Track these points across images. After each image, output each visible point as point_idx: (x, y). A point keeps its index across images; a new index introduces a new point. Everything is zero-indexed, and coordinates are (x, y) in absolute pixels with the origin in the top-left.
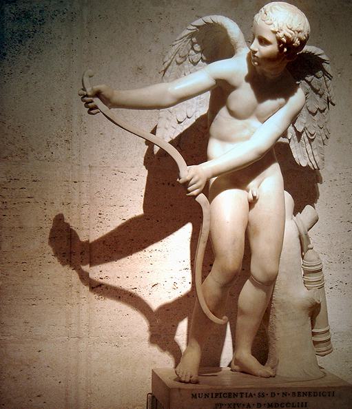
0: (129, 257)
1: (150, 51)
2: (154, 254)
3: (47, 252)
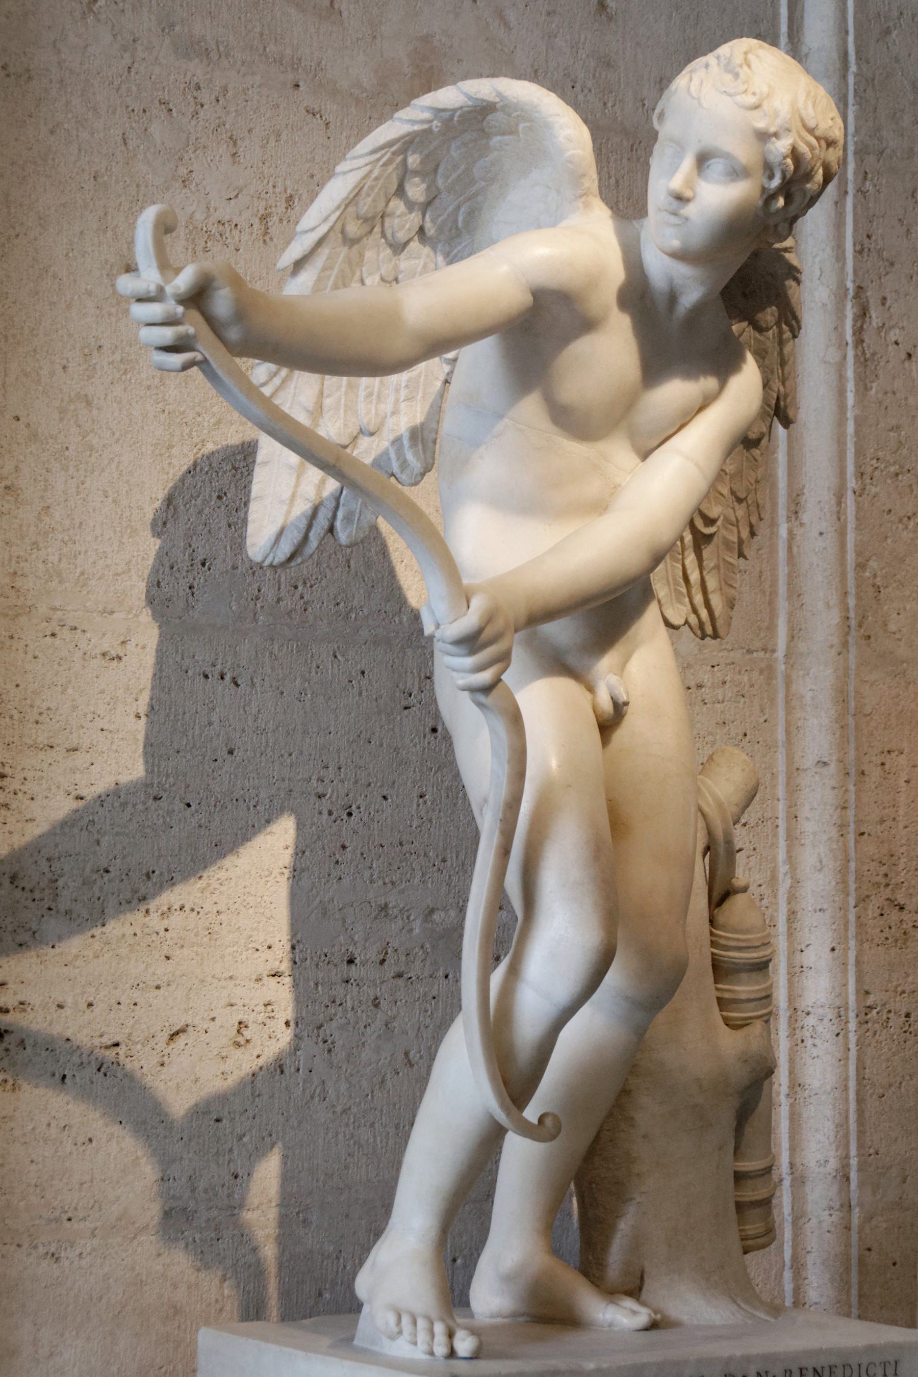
0: (97, 931)
2: (176, 920)
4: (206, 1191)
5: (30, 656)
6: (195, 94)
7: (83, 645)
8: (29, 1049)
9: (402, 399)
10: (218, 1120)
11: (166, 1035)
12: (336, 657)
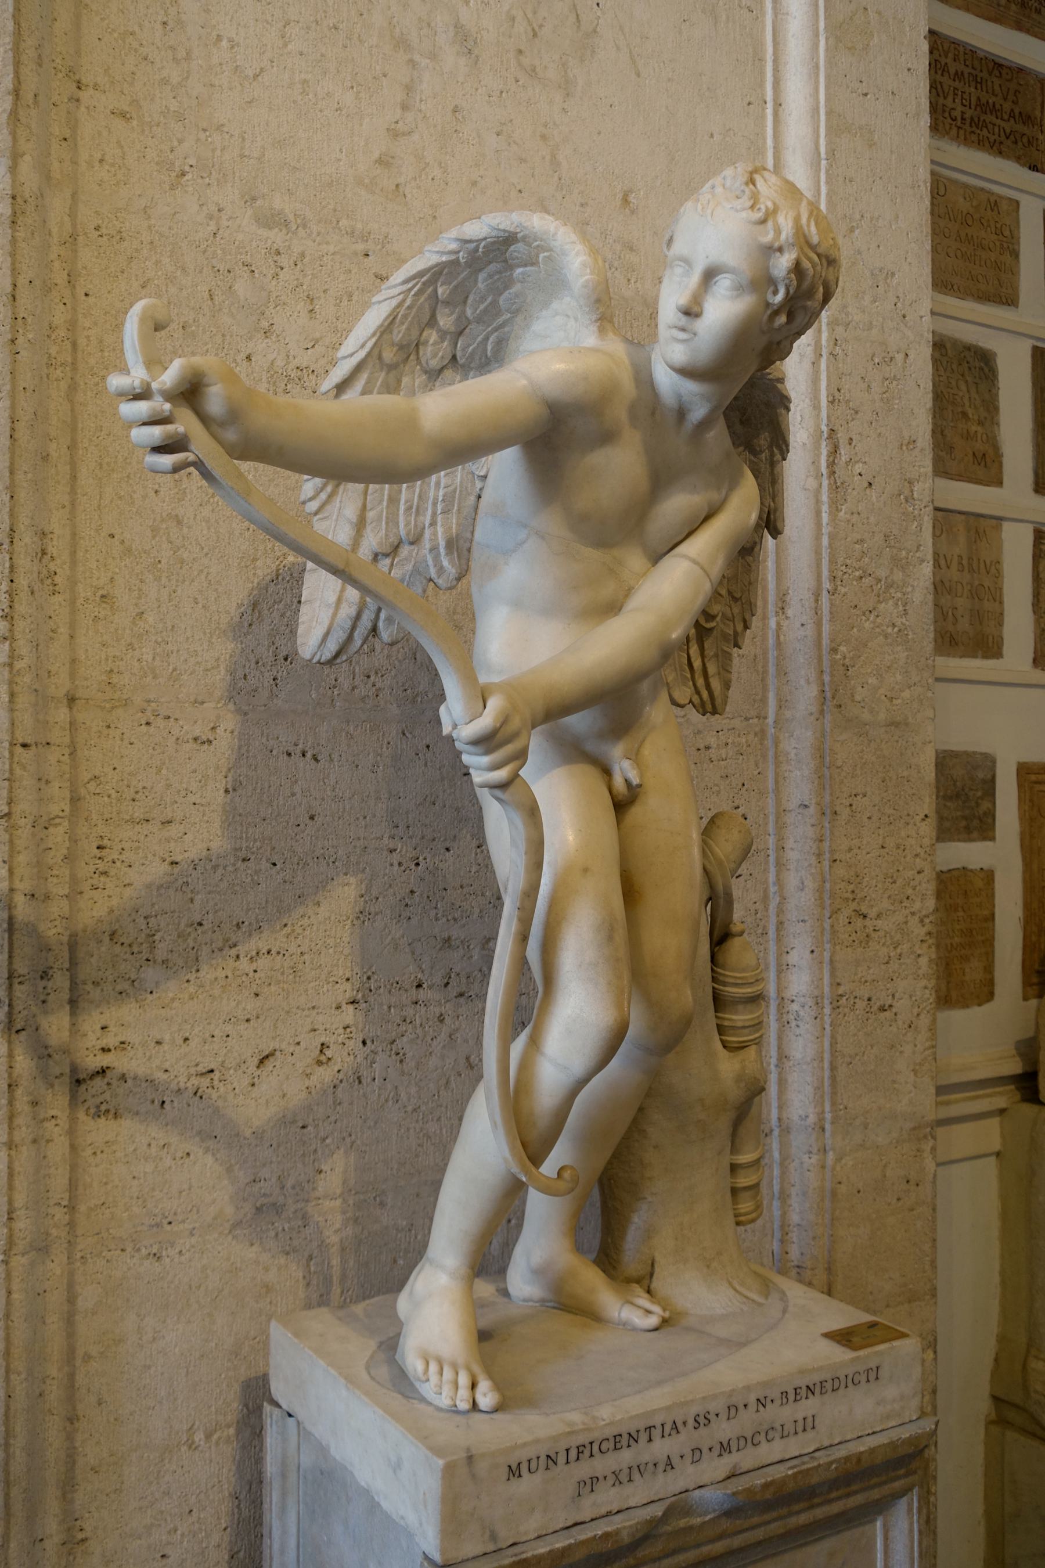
1: (249, 358)
2: (263, 962)
4: (293, 1188)
5: (126, 742)
6: (275, 258)
7: (176, 731)
8: (130, 1081)
9: (439, 512)
10: (303, 1127)
11: (256, 1061)
12: (404, 734)
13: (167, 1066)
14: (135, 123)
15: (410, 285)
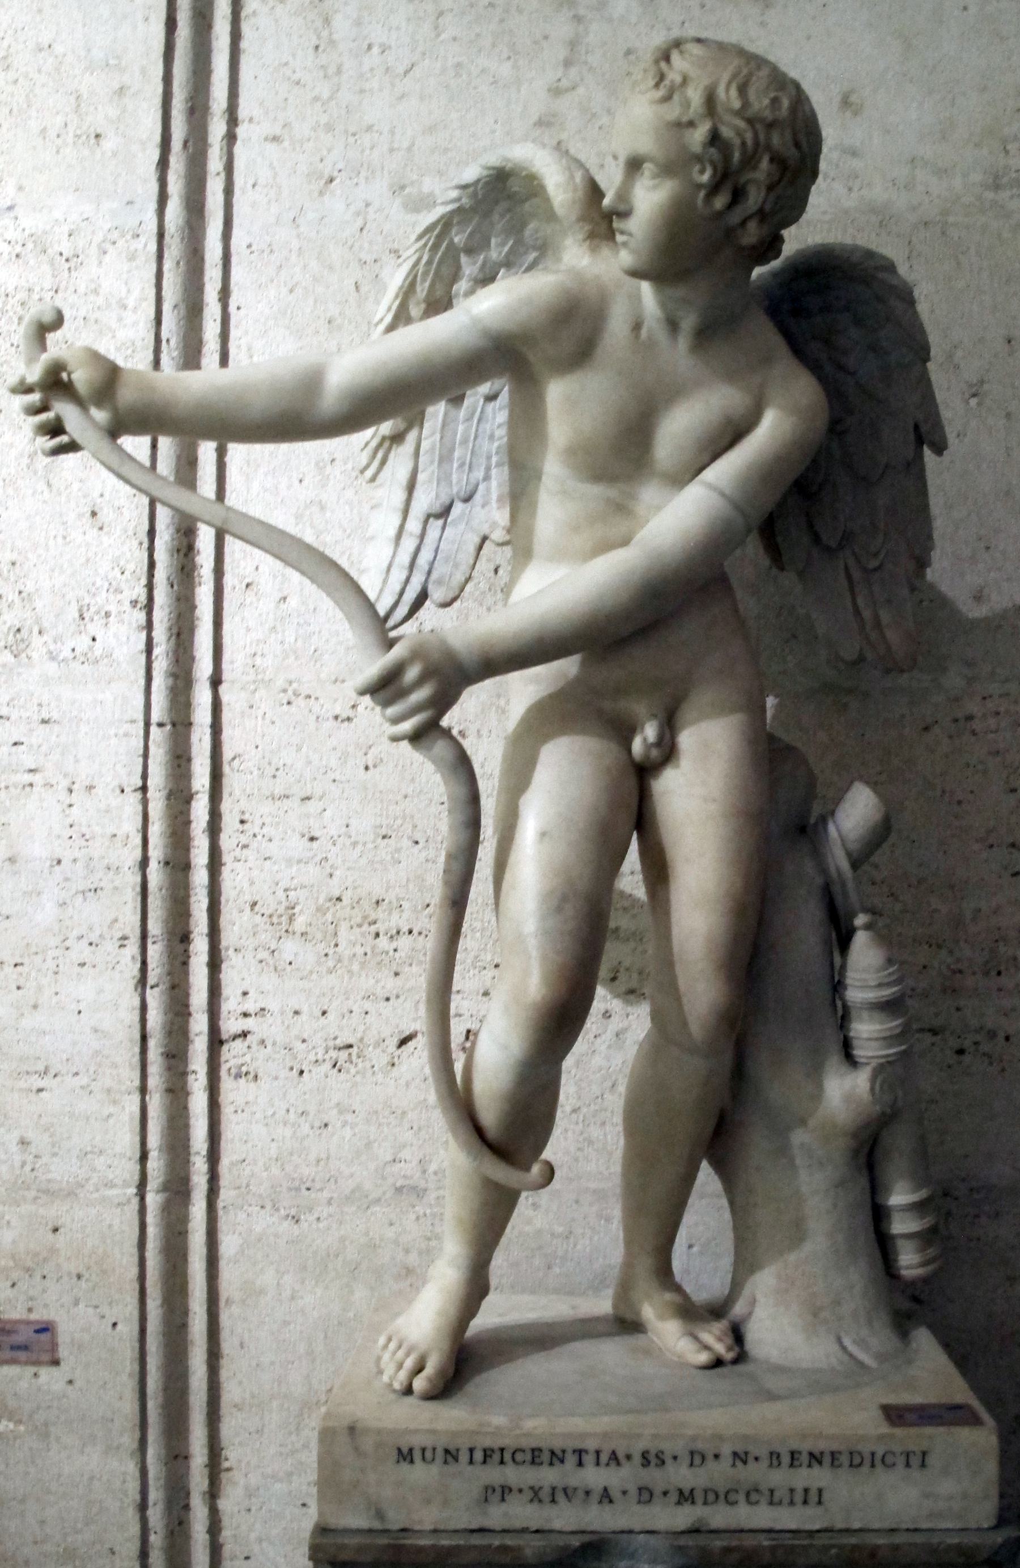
3: (75, 933)
4: (435, 1173)
5: (267, 721)
7: (316, 709)
8: (269, 1047)
11: (395, 1041)
13: (305, 1036)
14: (286, 144)
15: (423, 242)
